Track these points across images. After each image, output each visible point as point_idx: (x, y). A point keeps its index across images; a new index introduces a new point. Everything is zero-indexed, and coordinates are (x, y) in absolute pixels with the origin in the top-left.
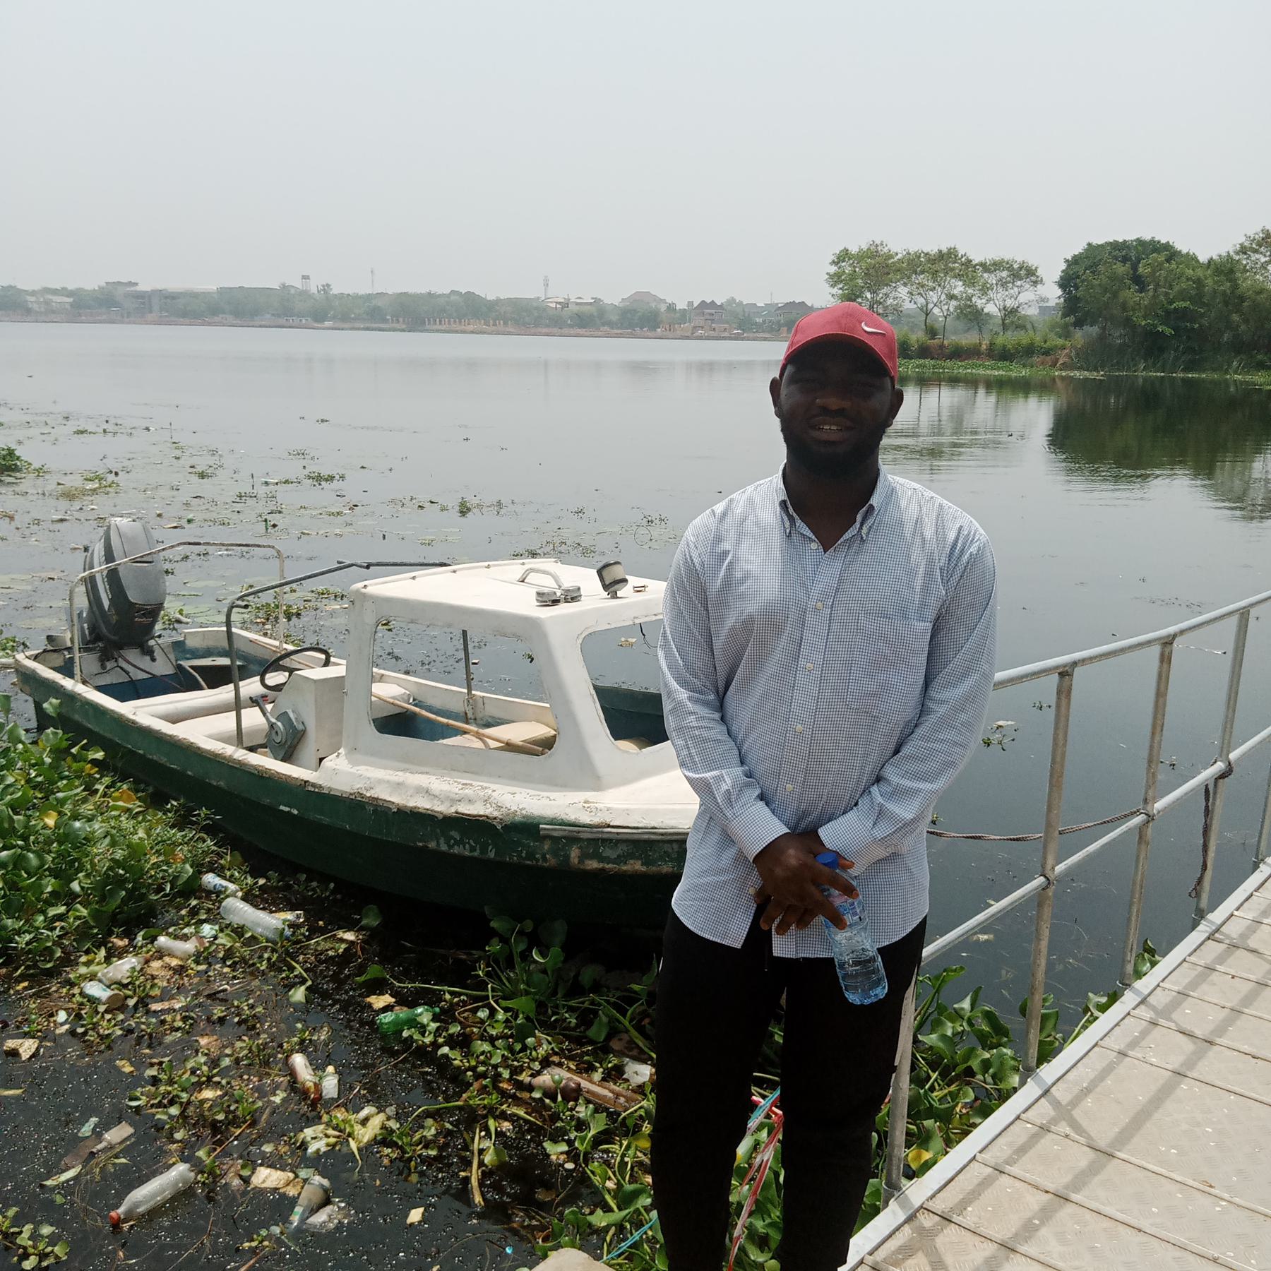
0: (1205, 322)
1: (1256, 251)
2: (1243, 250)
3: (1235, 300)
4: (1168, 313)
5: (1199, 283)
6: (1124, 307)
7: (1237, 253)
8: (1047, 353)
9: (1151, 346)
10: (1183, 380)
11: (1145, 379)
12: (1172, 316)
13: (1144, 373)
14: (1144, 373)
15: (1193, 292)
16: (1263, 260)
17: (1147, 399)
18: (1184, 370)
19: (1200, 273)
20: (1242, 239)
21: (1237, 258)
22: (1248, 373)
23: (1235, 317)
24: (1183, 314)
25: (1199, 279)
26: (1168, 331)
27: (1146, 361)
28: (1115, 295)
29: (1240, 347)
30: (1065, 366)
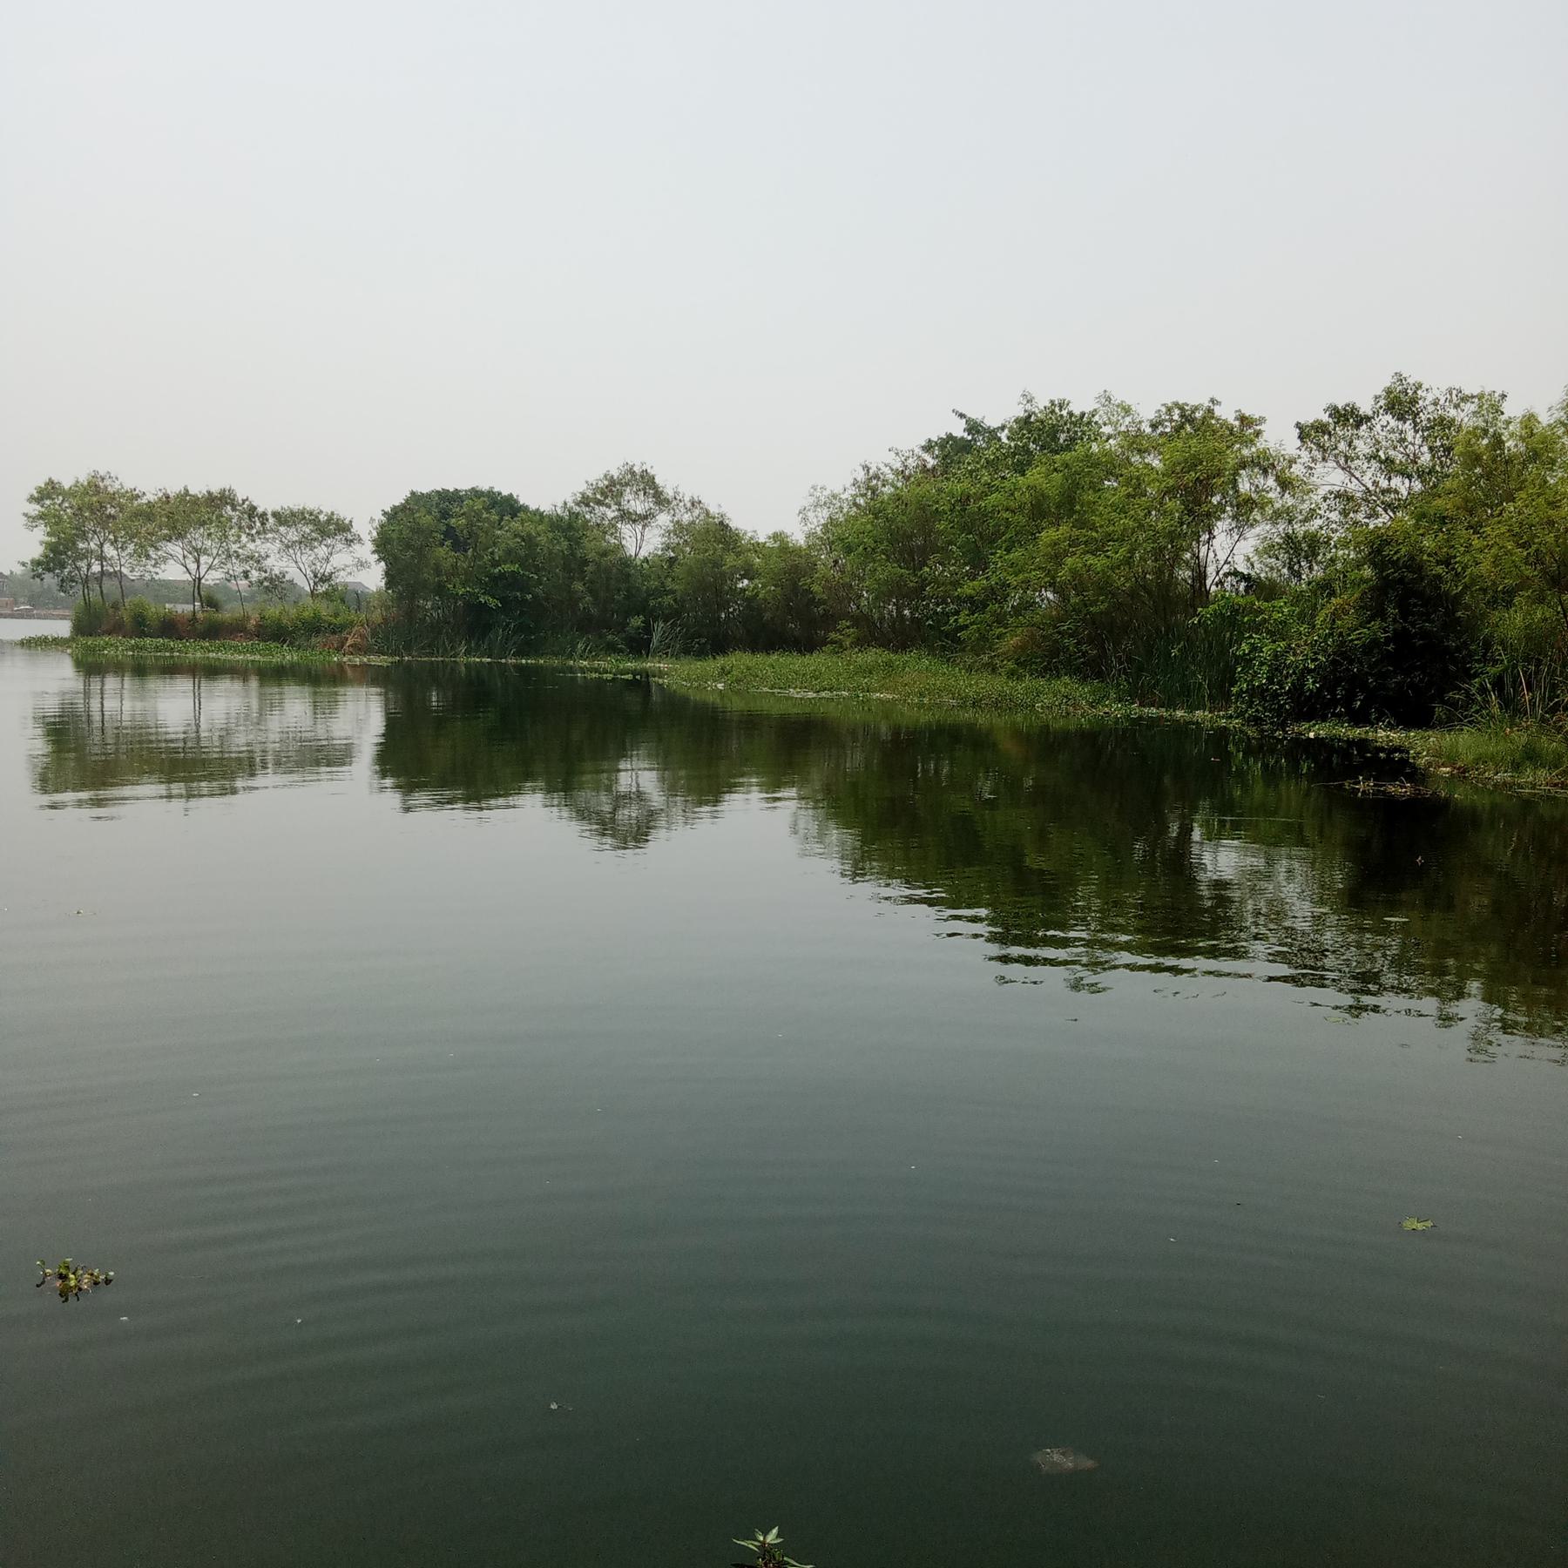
0: (539, 591)
1: (599, 503)
2: (585, 501)
3: (574, 564)
4: (496, 579)
5: (529, 541)
6: (437, 570)
7: (578, 504)
8: (335, 630)
9: (475, 623)
10: (519, 668)
11: (467, 666)
12: (498, 583)
13: (466, 659)
14: (466, 659)
15: (522, 553)
16: (611, 514)
17: (474, 694)
18: (520, 653)
19: (530, 528)
20: (583, 487)
21: (577, 509)
22: (595, 658)
23: (578, 586)
24: (513, 581)
25: (529, 535)
26: (493, 603)
27: (468, 642)
28: (420, 551)
29: (586, 625)
30: (358, 649)
